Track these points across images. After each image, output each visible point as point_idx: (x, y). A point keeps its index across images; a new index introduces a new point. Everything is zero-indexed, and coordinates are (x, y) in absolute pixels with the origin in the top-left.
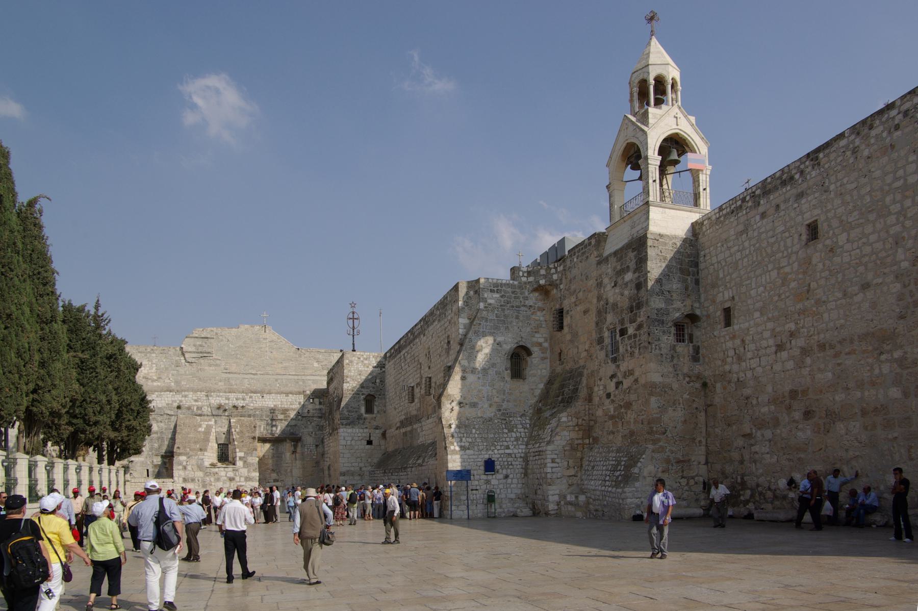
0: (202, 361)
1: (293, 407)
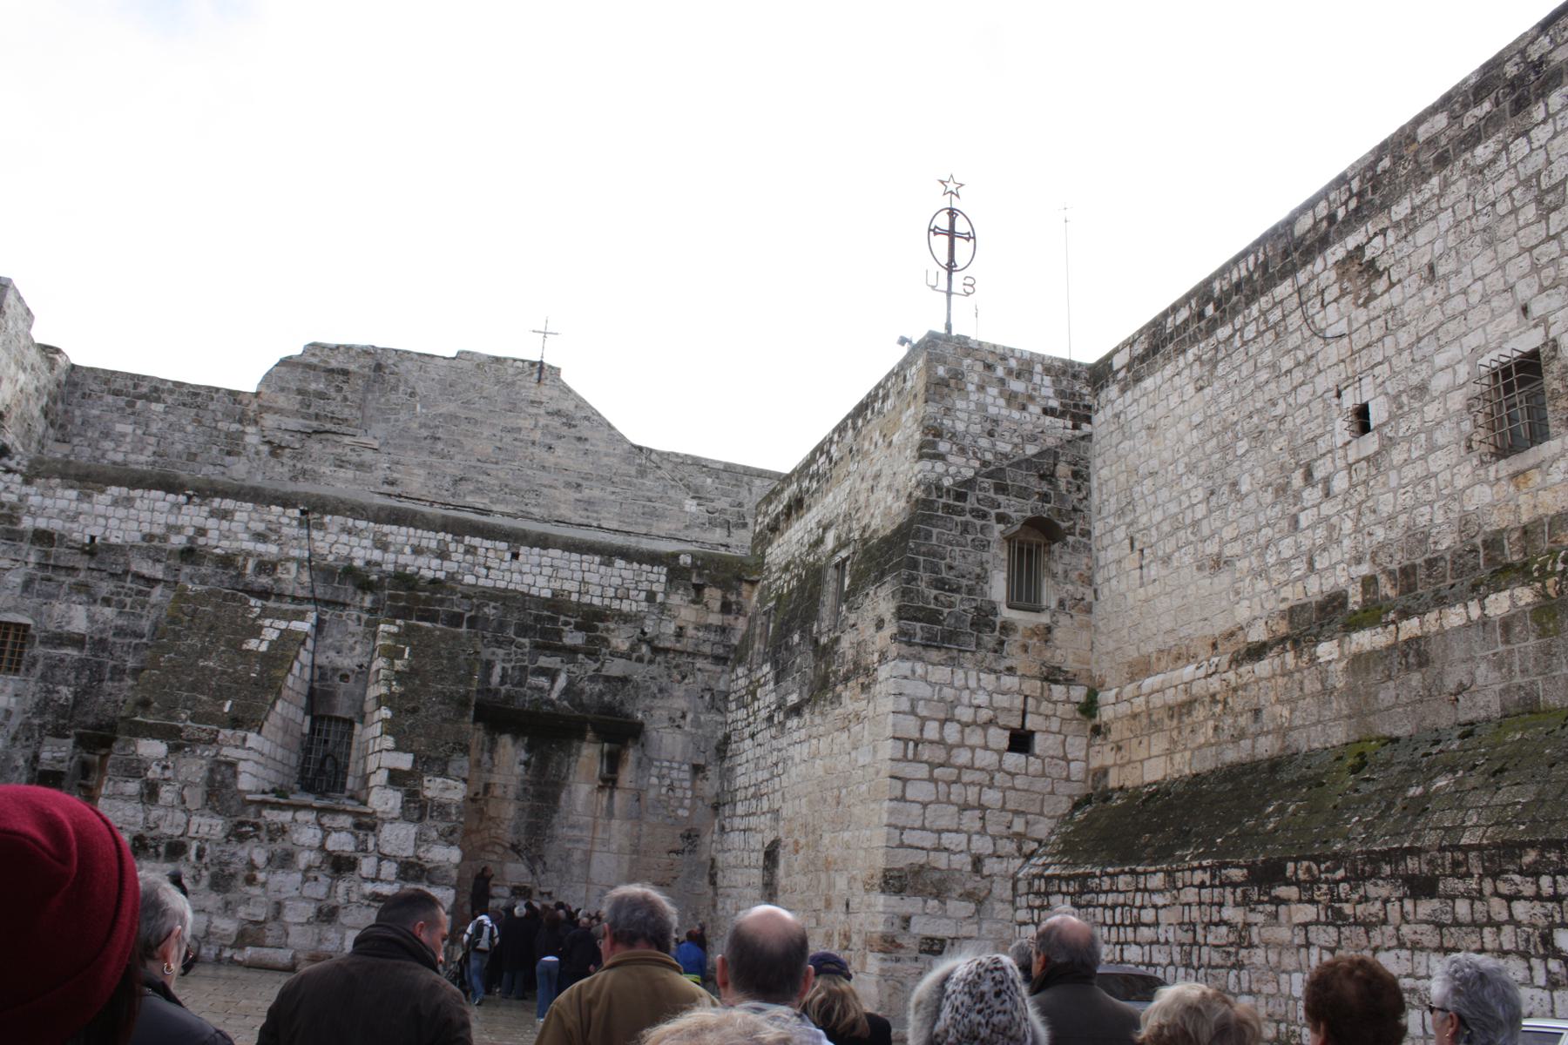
0: (315, 446)
1: (626, 606)
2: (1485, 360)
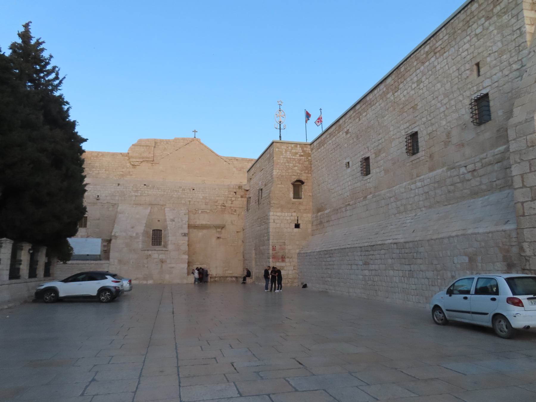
2: (363, 157)
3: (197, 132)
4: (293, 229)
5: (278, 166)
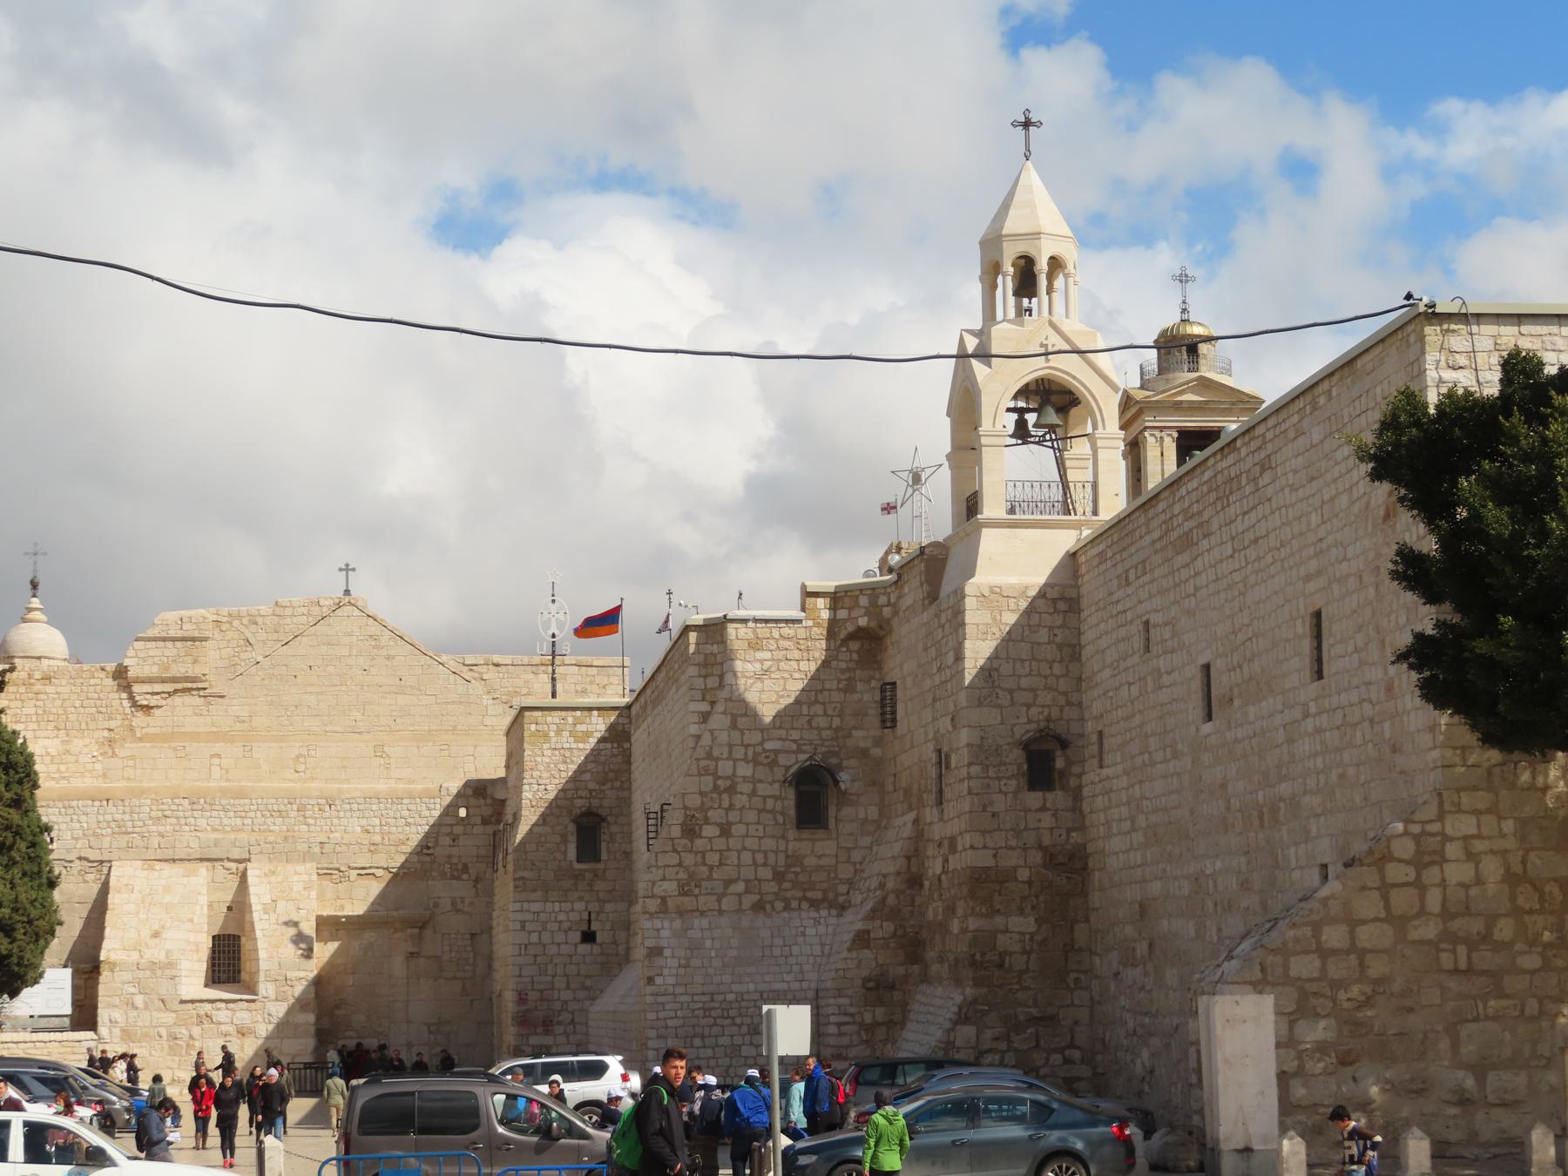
3: (354, 570)
4: (576, 945)
5: (536, 774)
